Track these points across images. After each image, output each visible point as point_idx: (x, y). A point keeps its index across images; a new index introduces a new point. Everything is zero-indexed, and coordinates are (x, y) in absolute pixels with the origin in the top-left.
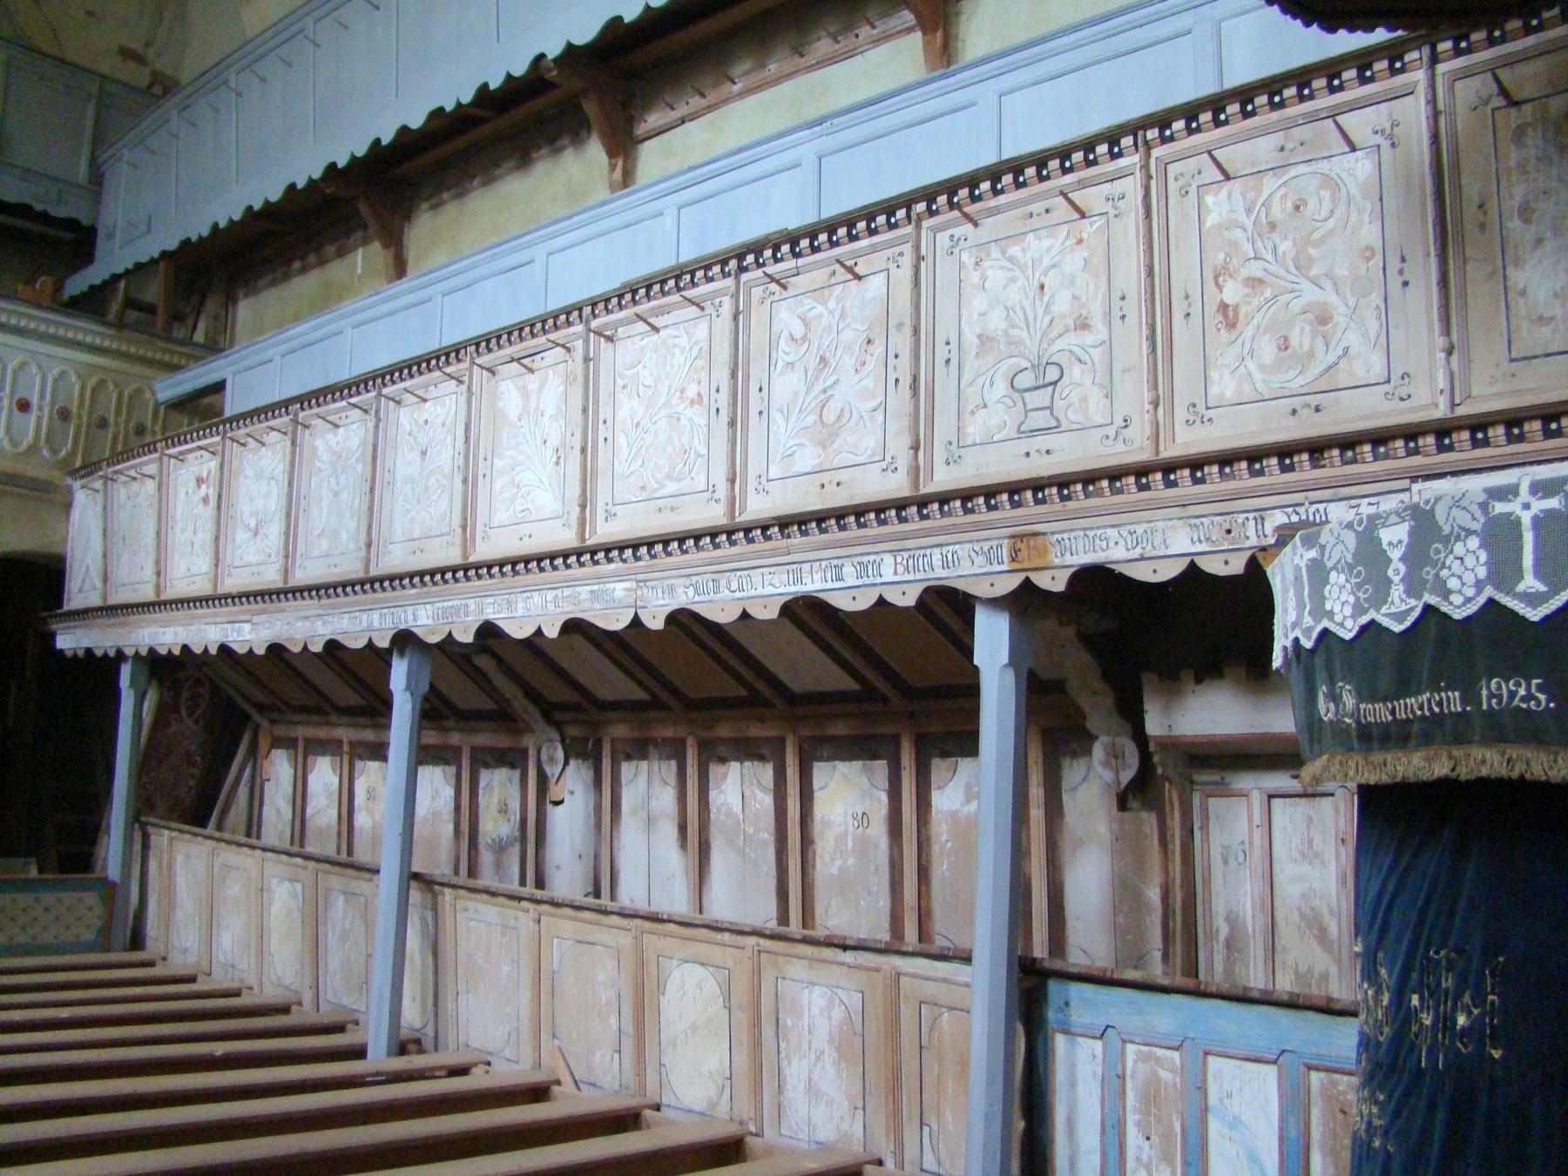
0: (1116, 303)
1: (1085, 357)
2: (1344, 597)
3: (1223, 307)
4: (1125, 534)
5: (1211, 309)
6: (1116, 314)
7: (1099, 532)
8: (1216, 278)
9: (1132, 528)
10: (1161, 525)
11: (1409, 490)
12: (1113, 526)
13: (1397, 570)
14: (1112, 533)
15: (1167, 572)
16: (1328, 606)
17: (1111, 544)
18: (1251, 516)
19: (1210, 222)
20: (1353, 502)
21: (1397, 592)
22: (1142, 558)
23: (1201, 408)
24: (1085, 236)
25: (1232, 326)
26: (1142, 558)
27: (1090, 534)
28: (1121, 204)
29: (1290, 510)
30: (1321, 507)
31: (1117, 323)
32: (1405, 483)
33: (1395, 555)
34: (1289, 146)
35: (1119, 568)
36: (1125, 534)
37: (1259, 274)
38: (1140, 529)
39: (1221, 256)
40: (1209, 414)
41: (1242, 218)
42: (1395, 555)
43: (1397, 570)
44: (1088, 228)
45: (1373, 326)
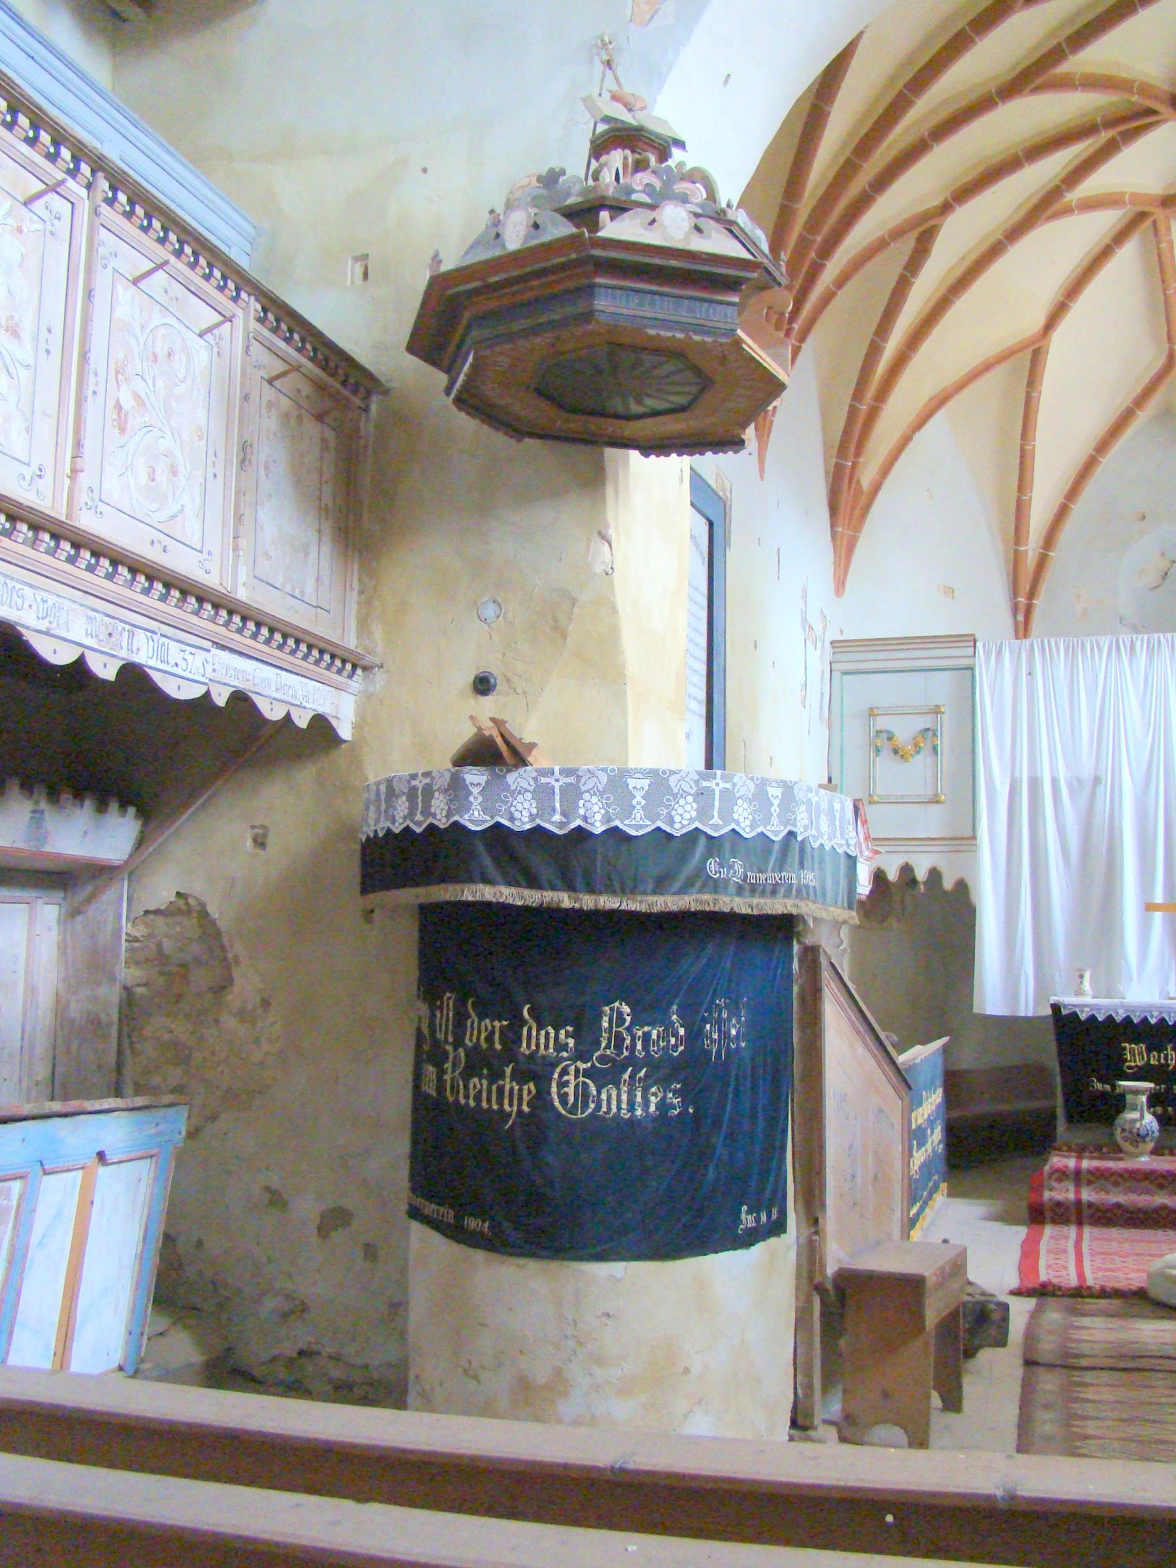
0: (44, 335)
1: (12, 370)
2: (746, 815)
3: (118, 407)
4: (39, 600)
5: (111, 403)
6: (43, 347)
7: (18, 586)
8: (117, 372)
9: (46, 595)
10: (67, 602)
11: (209, 651)
12: (31, 586)
13: (775, 810)
14: (28, 591)
15: (59, 655)
16: (735, 816)
17: (26, 606)
18: (127, 627)
19: (119, 313)
20: (184, 647)
21: (775, 820)
22: (47, 633)
23: (96, 496)
24: (25, 229)
25: (123, 430)
26: (47, 633)
27: (11, 584)
28: (56, 221)
29: (149, 634)
30: (167, 641)
31: (42, 355)
32: (208, 645)
33: (776, 802)
34: (171, 294)
35: (28, 636)
36: (39, 600)
37: (143, 396)
38: (52, 600)
39: (121, 355)
40: (102, 507)
41: (138, 331)
42: (776, 802)
43: (775, 810)
44: (31, 225)
45: (198, 500)
